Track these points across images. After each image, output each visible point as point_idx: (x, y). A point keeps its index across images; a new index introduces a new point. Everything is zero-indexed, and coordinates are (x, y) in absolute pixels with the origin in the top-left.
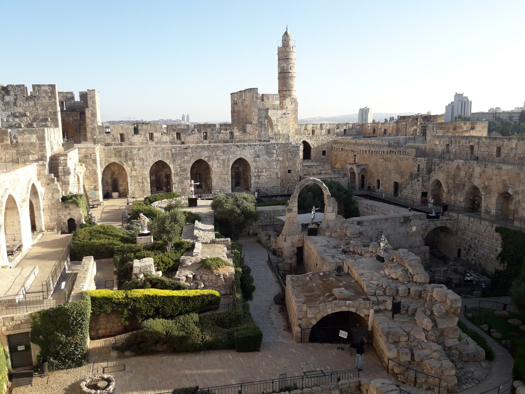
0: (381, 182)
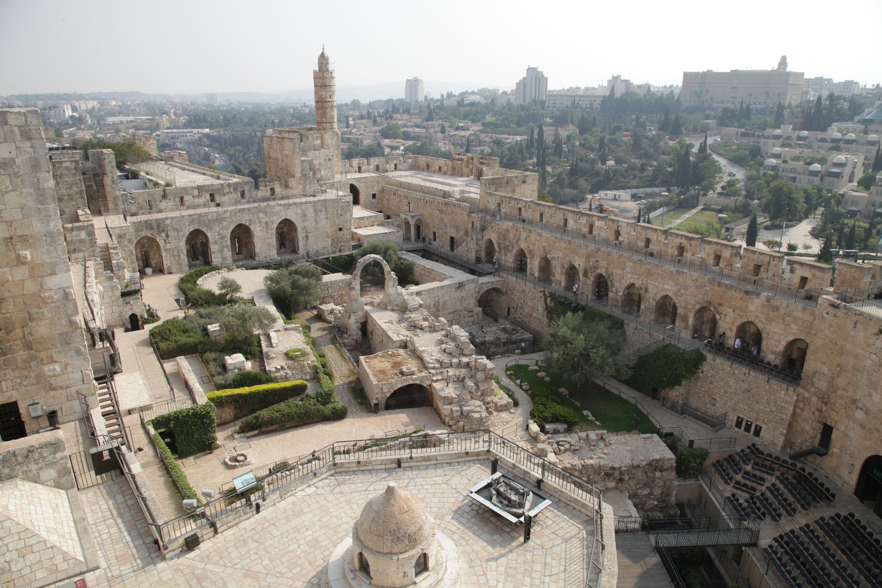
0: (437, 234)
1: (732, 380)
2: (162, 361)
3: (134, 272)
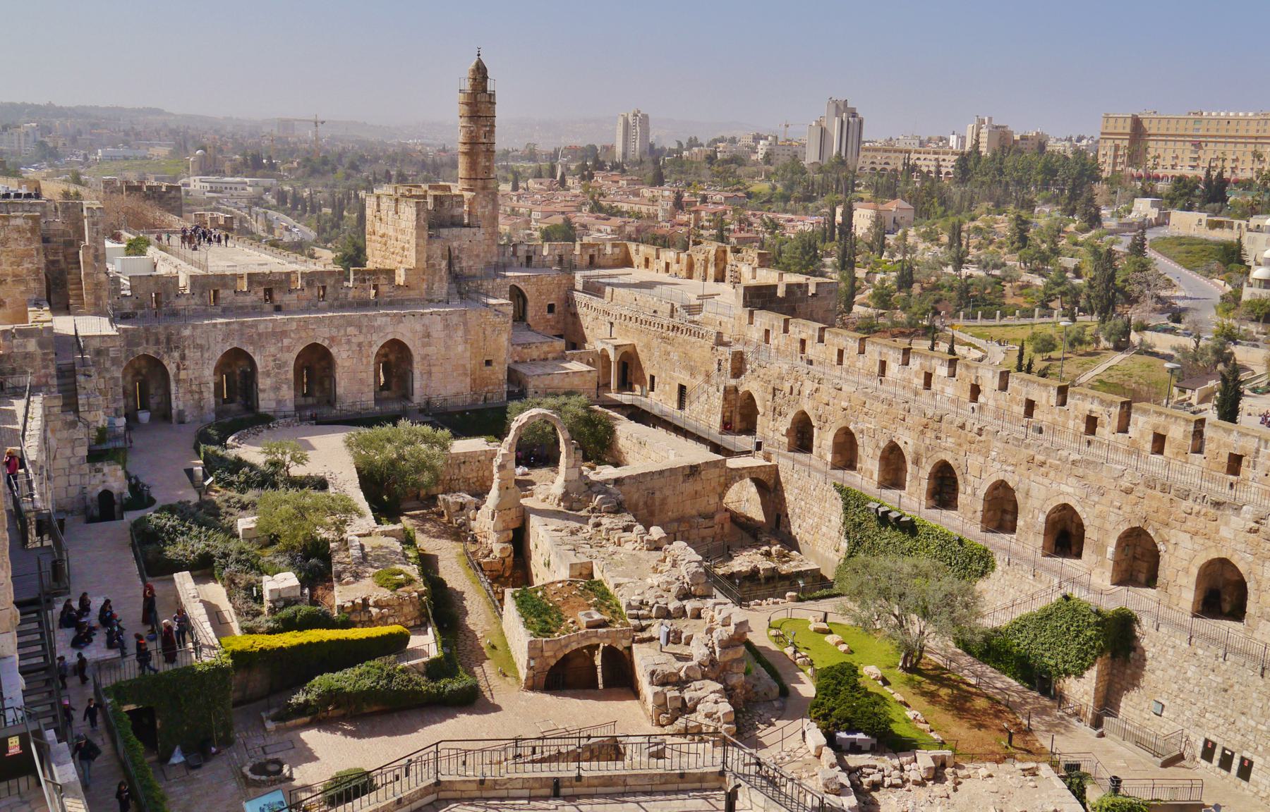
0: (656, 380)
1: (1193, 668)
2: (148, 579)
3: (118, 416)
